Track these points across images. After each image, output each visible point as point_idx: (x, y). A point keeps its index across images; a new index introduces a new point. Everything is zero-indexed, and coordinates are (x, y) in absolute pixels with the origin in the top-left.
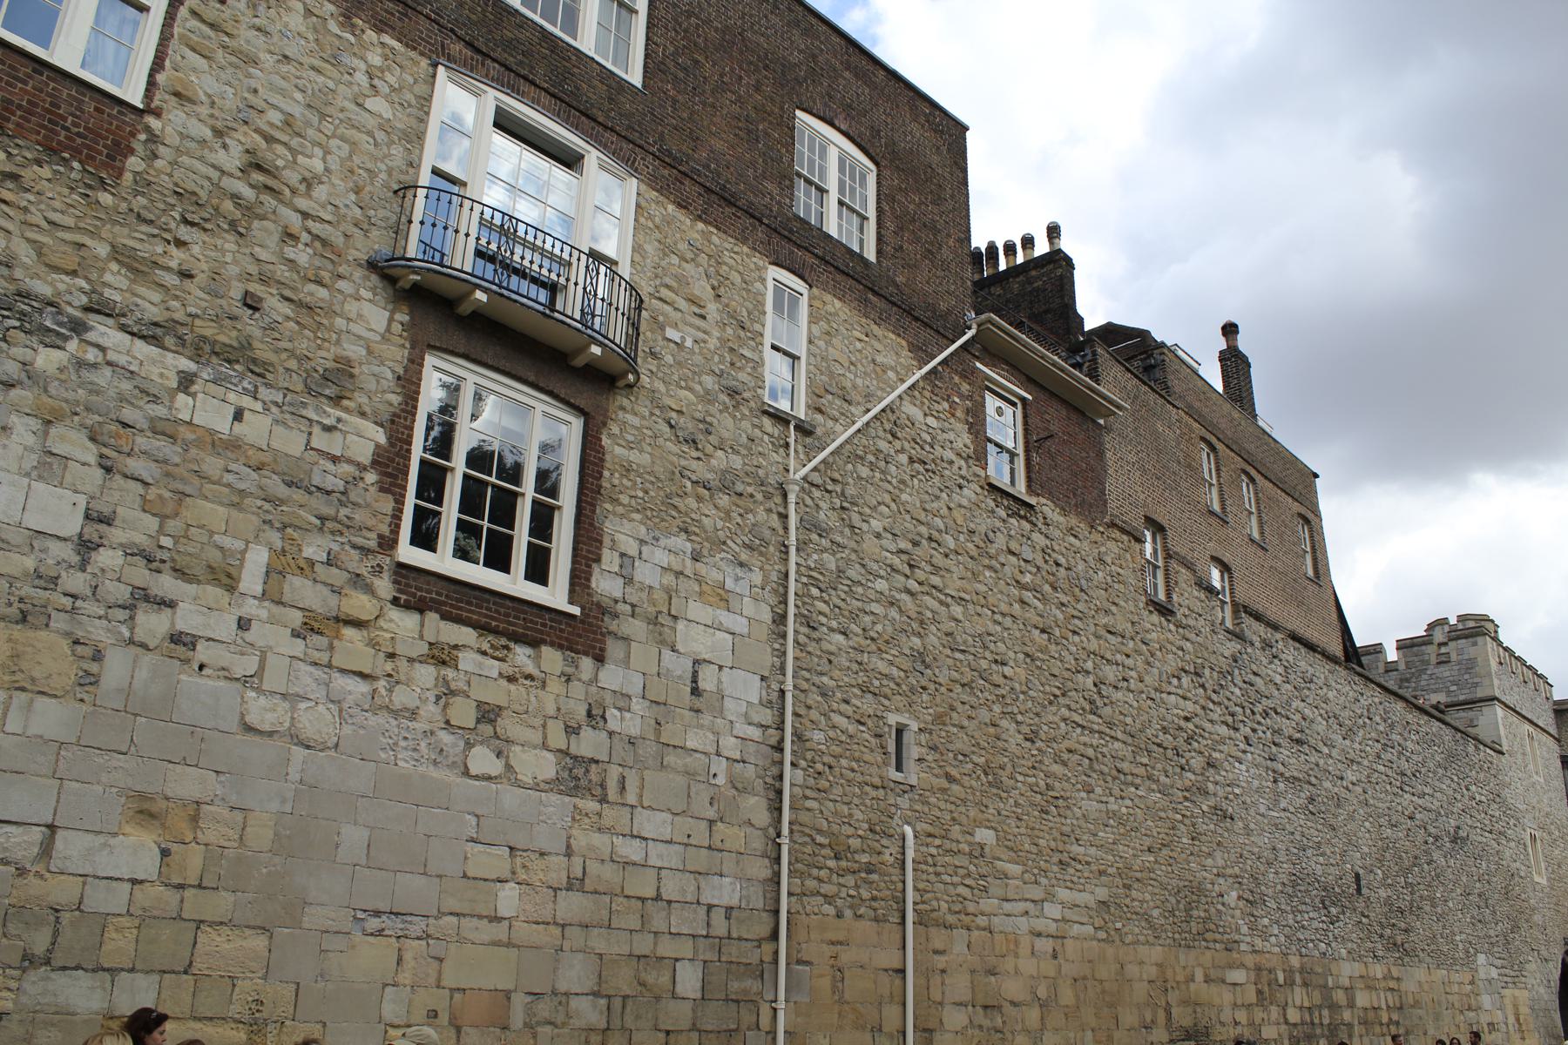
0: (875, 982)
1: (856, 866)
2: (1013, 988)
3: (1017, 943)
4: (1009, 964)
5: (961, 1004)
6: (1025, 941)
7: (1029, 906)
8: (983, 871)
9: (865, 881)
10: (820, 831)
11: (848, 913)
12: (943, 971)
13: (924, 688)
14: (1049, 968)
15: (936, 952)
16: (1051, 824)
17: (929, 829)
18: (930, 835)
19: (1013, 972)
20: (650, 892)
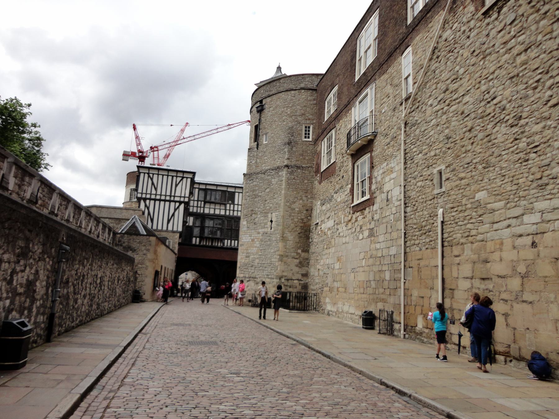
0: (431, 272)
1: (424, 232)
2: (497, 268)
3: (502, 244)
4: (496, 256)
5: (467, 278)
6: (508, 243)
7: (513, 222)
8: (480, 212)
9: (428, 235)
10: (415, 224)
11: (424, 249)
12: (459, 264)
13: (449, 148)
14: (529, 254)
15: (456, 256)
16: (529, 166)
17: (451, 205)
18: (452, 208)
19: (498, 259)
20: (381, 255)
